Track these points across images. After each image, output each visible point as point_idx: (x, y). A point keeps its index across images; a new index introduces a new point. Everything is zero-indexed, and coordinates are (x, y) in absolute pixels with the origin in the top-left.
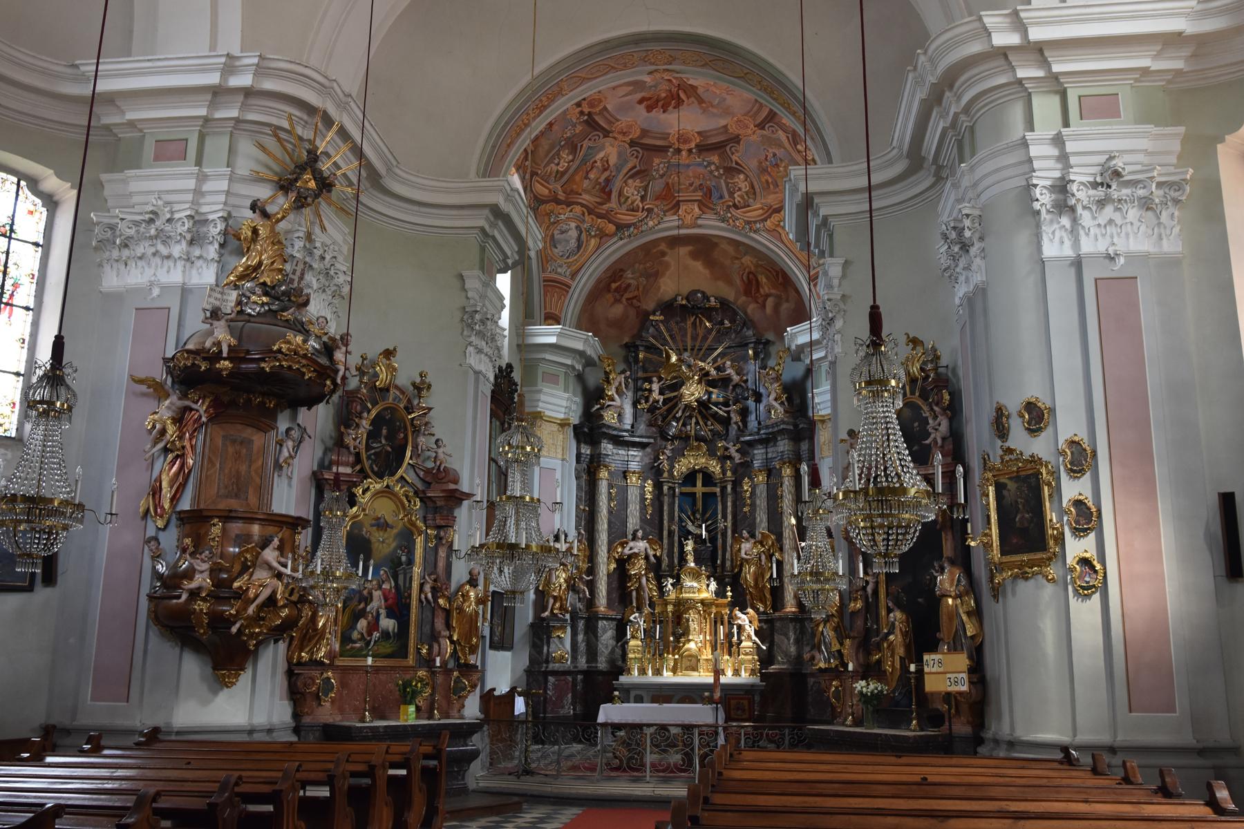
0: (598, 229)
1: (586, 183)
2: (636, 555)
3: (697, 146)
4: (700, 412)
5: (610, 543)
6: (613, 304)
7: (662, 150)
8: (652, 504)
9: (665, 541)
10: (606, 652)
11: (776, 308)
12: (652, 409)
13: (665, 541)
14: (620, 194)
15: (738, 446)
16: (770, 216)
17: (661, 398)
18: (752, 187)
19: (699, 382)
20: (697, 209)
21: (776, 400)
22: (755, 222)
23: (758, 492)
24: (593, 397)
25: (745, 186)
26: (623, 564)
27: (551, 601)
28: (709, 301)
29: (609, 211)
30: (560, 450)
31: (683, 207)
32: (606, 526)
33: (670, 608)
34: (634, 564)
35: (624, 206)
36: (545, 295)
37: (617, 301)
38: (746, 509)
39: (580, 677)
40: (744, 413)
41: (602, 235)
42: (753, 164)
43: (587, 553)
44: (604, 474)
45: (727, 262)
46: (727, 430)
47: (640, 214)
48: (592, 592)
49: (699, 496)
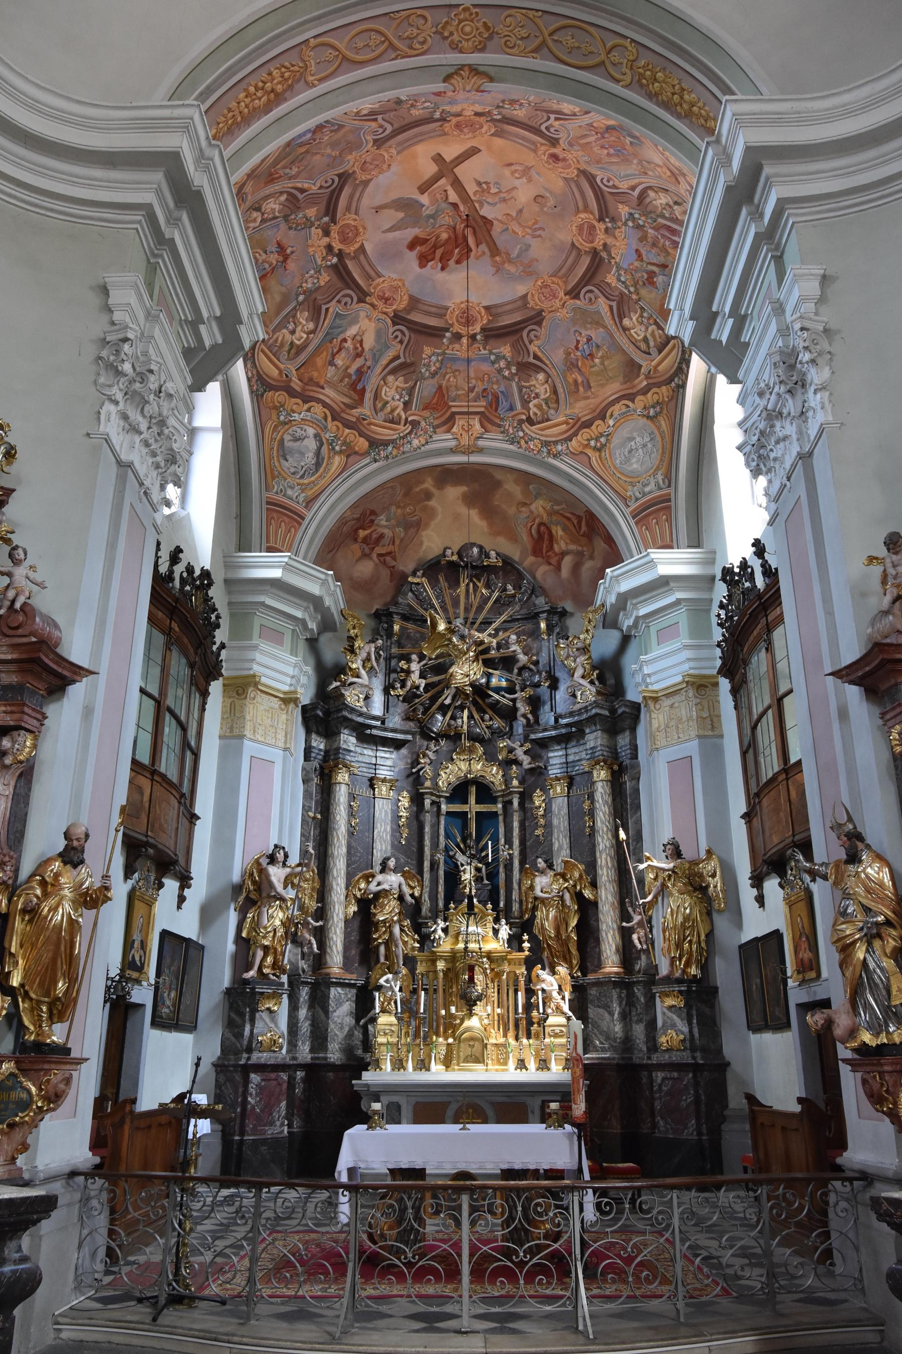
2: (385, 893)
3: (483, 329)
4: (475, 703)
8: (408, 825)
9: (427, 876)
10: (341, 1035)
11: (576, 569)
12: (409, 698)
13: (427, 876)
14: (377, 396)
15: (528, 745)
16: (575, 434)
17: (423, 683)
18: (555, 392)
19: (476, 659)
20: (477, 426)
21: (583, 677)
22: (556, 443)
23: (555, 808)
24: (329, 675)
25: (543, 390)
26: (366, 905)
27: (260, 954)
28: (488, 556)
29: (362, 419)
30: (281, 736)
31: (460, 422)
32: (344, 850)
33: (441, 965)
34: (383, 906)
35: (381, 415)
37: (365, 556)
38: (538, 832)
39: (300, 1074)
40: (535, 703)
41: (350, 453)
42: (557, 357)
43: (317, 885)
44: (342, 777)
45: (512, 511)
46: (511, 728)
47: (401, 427)
48: (322, 945)
49: (472, 816)
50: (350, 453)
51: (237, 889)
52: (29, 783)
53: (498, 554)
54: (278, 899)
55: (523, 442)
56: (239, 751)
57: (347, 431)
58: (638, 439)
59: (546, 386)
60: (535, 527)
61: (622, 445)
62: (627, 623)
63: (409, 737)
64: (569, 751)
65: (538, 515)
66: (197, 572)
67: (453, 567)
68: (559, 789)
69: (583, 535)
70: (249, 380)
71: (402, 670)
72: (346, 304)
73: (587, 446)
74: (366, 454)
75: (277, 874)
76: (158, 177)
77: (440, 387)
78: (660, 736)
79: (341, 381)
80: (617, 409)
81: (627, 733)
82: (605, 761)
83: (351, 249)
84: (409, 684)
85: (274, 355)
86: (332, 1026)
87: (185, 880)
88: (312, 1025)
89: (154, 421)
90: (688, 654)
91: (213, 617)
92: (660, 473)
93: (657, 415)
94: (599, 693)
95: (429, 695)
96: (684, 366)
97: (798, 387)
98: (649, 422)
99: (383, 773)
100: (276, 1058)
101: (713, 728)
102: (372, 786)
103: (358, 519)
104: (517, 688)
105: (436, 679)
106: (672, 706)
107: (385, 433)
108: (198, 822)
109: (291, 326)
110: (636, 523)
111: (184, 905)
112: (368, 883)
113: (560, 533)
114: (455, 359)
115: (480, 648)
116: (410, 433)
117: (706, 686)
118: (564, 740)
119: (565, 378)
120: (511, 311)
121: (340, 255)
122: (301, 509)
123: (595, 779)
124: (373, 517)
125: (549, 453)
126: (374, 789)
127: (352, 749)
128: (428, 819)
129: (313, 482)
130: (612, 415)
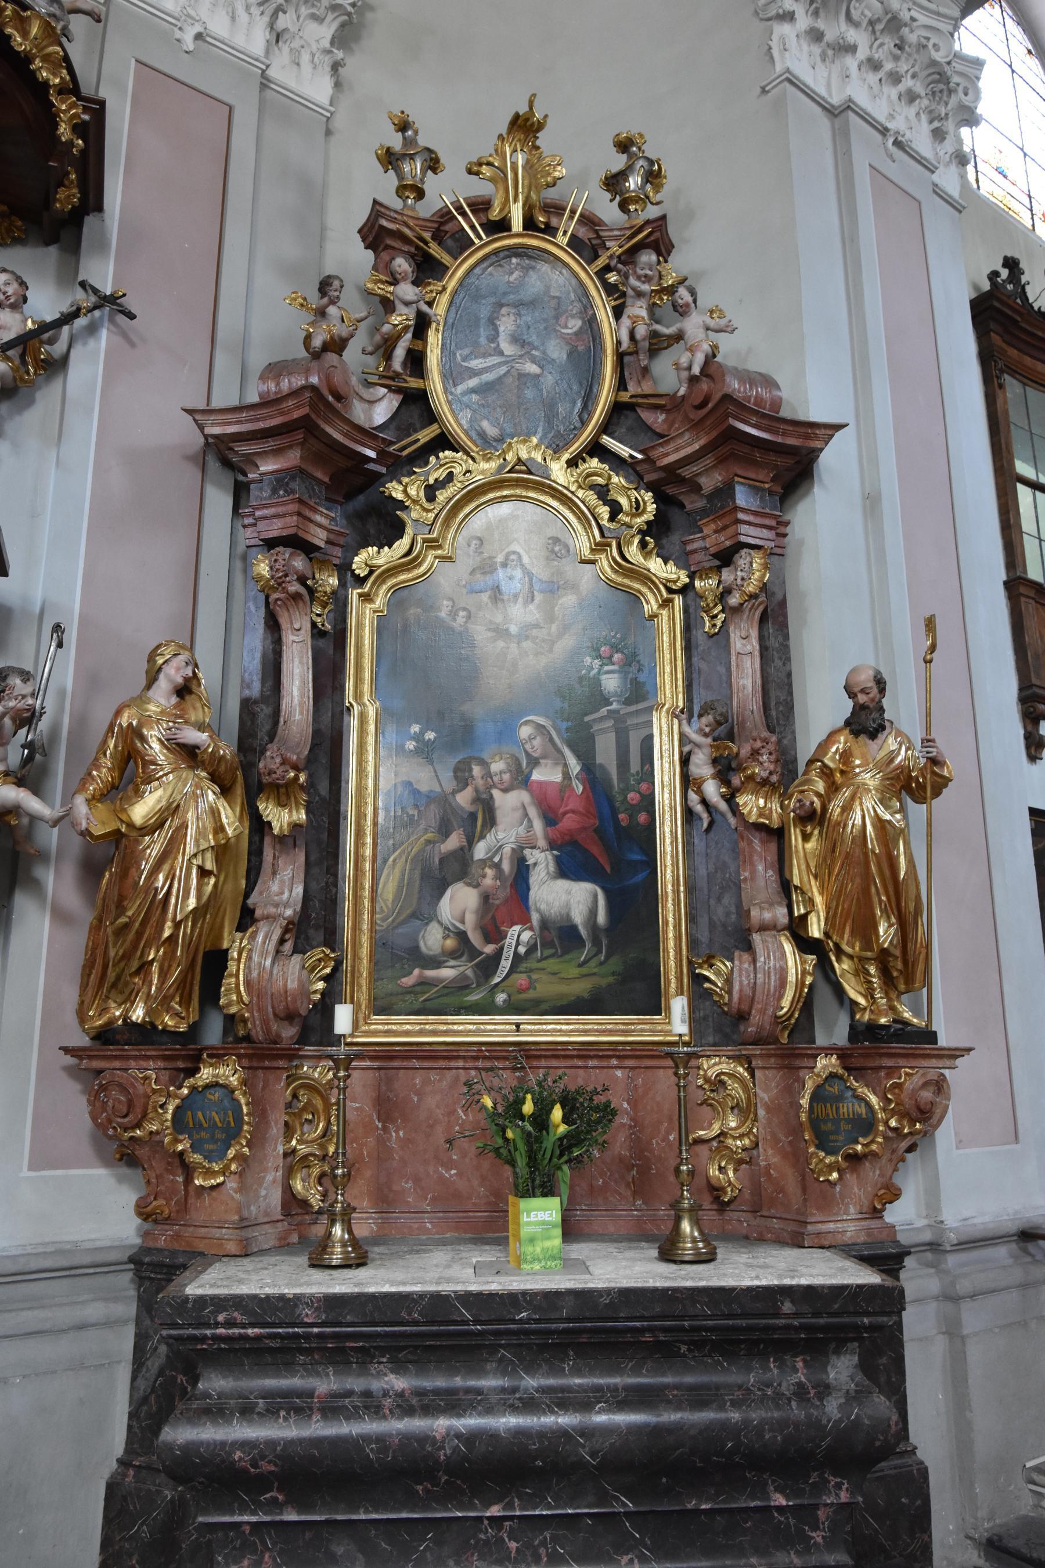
52: (783, 626)
89: (879, 27)
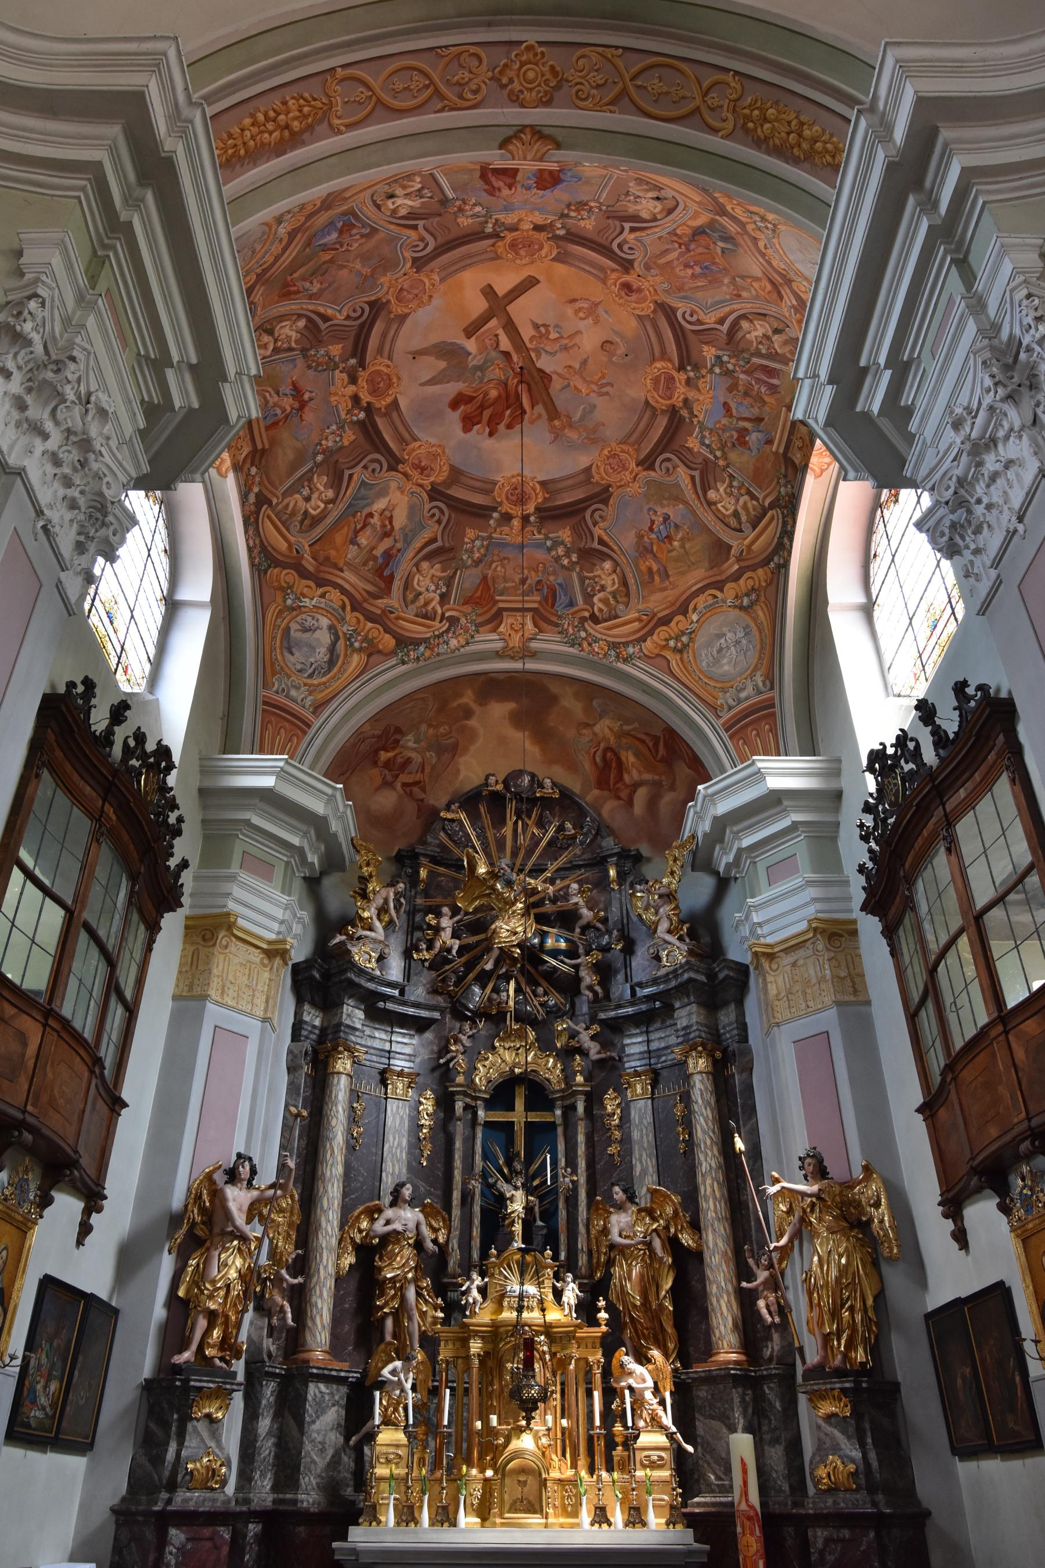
0: (365, 639)
1: (352, 551)
3: (538, 509)
5: (346, 1211)
6: (378, 789)
7: (479, 513)
8: (432, 1138)
9: (456, 1212)
10: (321, 1462)
11: (652, 803)
12: (439, 963)
13: (456, 1212)
14: (407, 585)
15: (596, 1028)
16: (651, 633)
17: (456, 944)
18: (624, 583)
21: (669, 932)
22: (626, 644)
23: (634, 1115)
24: (331, 927)
26: (369, 1254)
27: (202, 1323)
28: (541, 786)
29: (387, 612)
30: (260, 1001)
31: (508, 620)
32: (339, 1169)
33: (476, 1346)
34: (393, 1257)
35: (413, 608)
36: (264, 729)
37: (387, 784)
38: (612, 1150)
39: (253, 1529)
41: (372, 651)
42: (627, 541)
43: (296, 1219)
44: (343, 1064)
45: (571, 733)
46: (573, 1006)
47: (436, 624)
50: (372, 651)
51: (175, 1220)
53: (554, 784)
54: (236, 1237)
55: (585, 644)
56: (198, 1018)
57: (370, 625)
58: (729, 635)
59: (614, 576)
60: (599, 753)
61: (709, 644)
62: (724, 860)
63: (436, 1015)
64: (652, 1036)
65: (604, 738)
66: (150, 746)
67: (497, 801)
68: (639, 1091)
69: (661, 761)
70: (250, 550)
71: (430, 927)
72: (373, 471)
73: (665, 647)
74: (393, 653)
75: (237, 1198)
76: (115, 131)
77: (485, 578)
78: (781, 1006)
79: (365, 564)
80: (701, 601)
81: (732, 1006)
82: (703, 1045)
83: (382, 403)
84: (438, 945)
85: (283, 524)
86: (308, 1446)
87: (93, 1198)
88: (278, 1445)
89: (73, 438)
90: (812, 892)
91: (172, 819)
92: (759, 673)
93: (752, 605)
94: (691, 952)
95: (463, 959)
96: (786, 540)
97: (1024, 390)
98: (742, 614)
99: (399, 1064)
100: (214, 1500)
101: (855, 992)
102: (384, 1082)
103: (379, 737)
104: (581, 951)
105: (472, 940)
106: (794, 964)
107: (416, 630)
108: (124, 1112)
109: (306, 492)
110: (731, 737)
111: (89, 1240)
112: (373, 1220)
113: (632, 759)
114: (504, 545)
115: (532, 900)
116: (447, 631)
117: (842, 936)
118: (644, 1020)
119: (637, 566)
120: (572, 487)
121: (369, 409)
122: (308, 715)
123: (691, 1070)
124: (398, 737)
125: (618, 657)
126: (386, 1087)
127: (359, 1026)
128: (459, 1129)
129: (324, 683)
130: (695, 609)
